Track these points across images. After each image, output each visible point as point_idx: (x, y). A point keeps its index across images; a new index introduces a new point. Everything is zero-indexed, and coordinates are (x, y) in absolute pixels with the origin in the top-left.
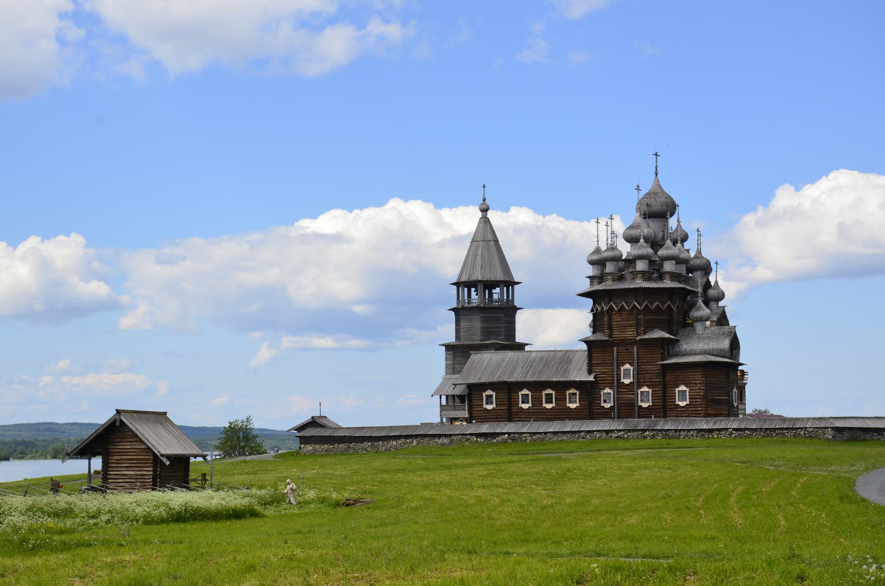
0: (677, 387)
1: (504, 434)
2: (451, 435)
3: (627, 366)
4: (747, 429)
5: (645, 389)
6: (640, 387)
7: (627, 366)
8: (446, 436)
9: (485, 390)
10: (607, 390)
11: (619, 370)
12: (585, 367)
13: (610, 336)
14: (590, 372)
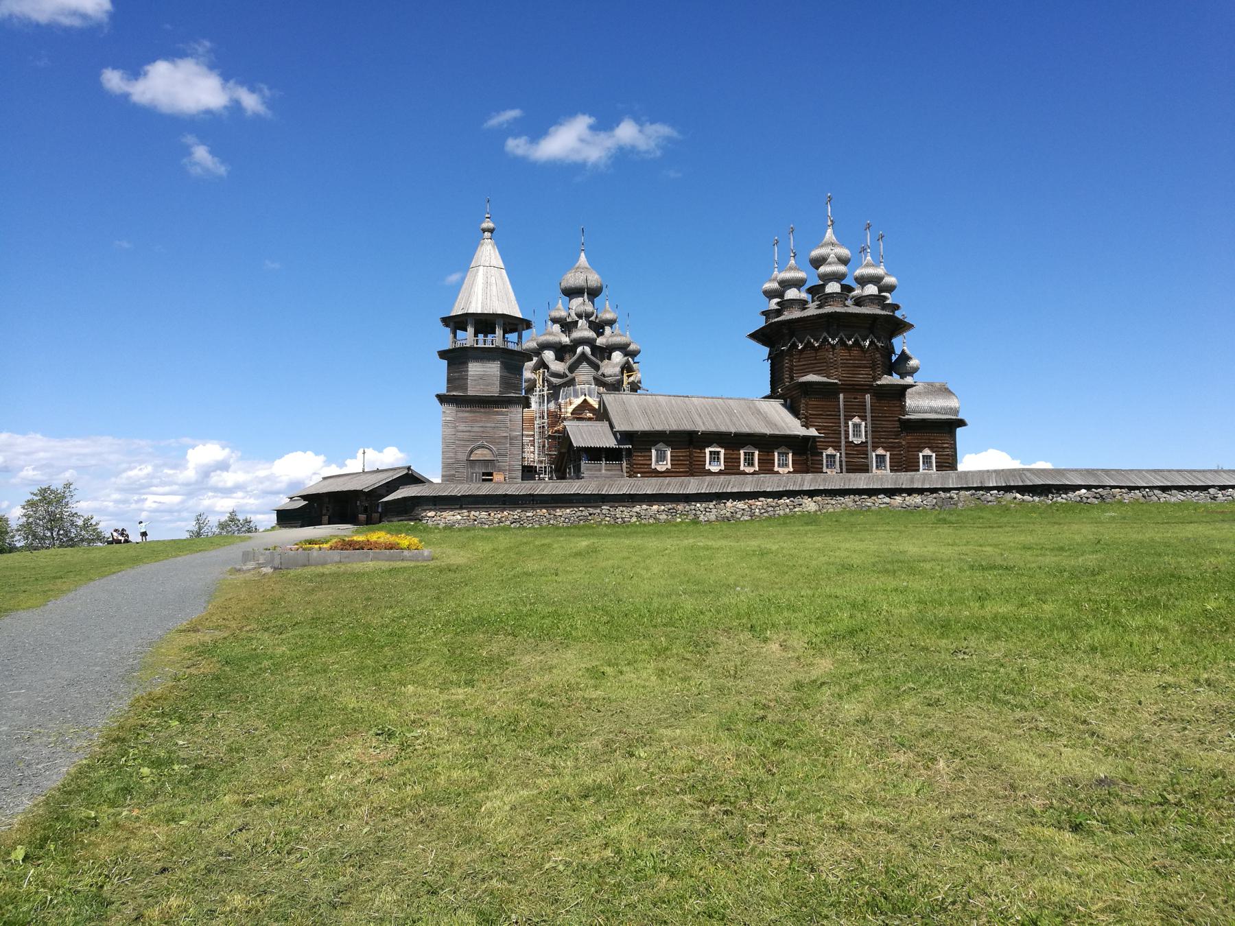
1: (1079, 487)
2: (934, 491)
3: (856, 420)
5: (880, 451)
6: (875, 448)
7: (856, 420)
8: (920, 491)
10: (830, 451)
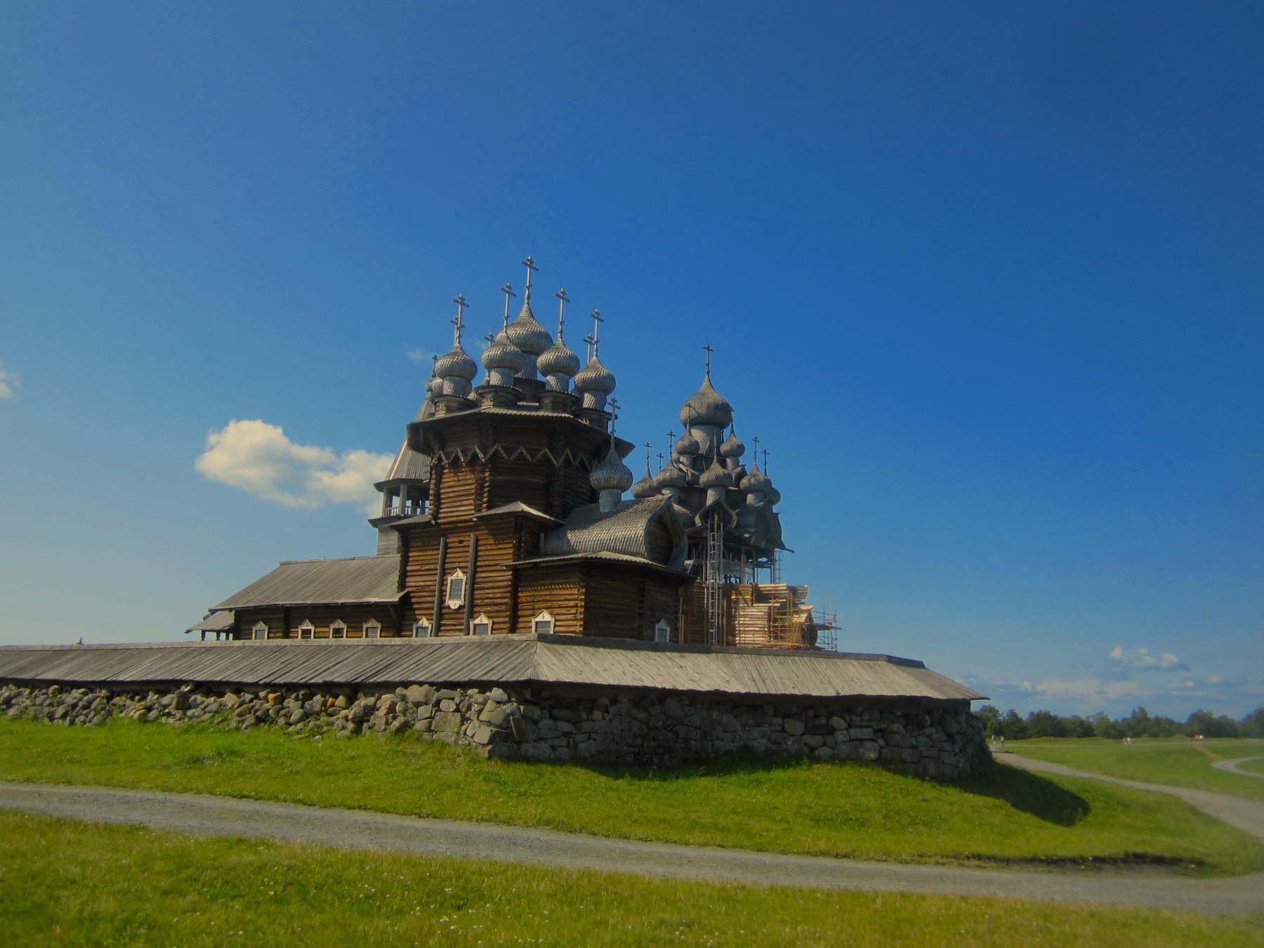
0: (533, 615)
3: (459, 574)
4: (238, 688)
5: (483, 619)
7: (459, 574)
9: (255, 622)
11: (442, 582)
12: (395, 577)
13: (436, 515)
14: (402, 585)
